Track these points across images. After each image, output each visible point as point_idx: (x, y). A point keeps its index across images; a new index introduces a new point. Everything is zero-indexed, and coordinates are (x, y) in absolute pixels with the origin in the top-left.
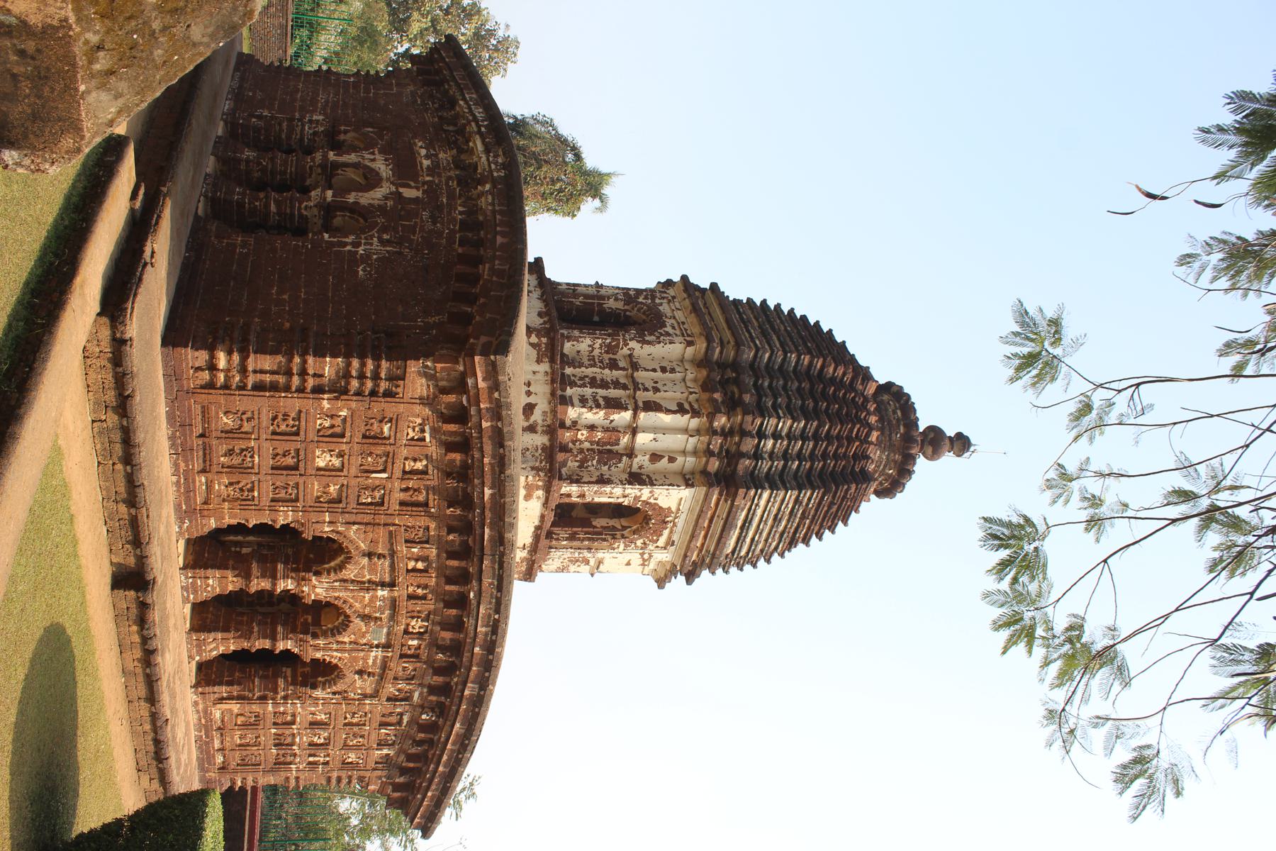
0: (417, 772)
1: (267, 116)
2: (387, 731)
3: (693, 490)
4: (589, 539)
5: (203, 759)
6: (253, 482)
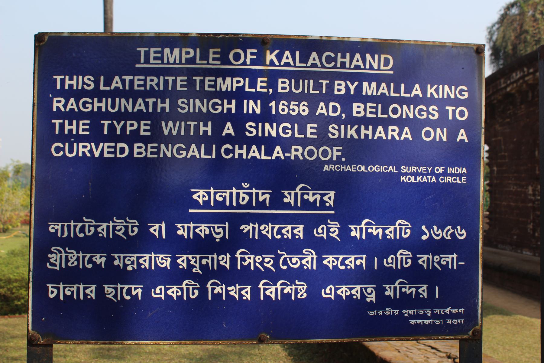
1: (533, 226)
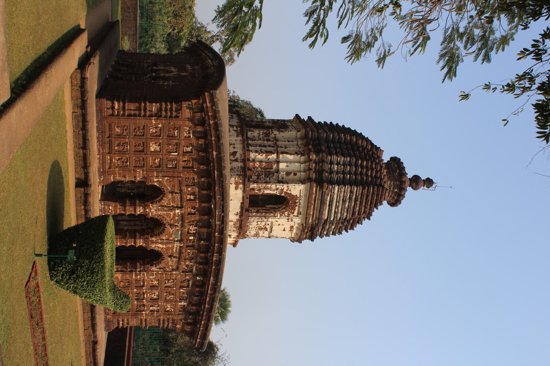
0: (197, 313)
2: (183, 291)
3: (305, 185)
4: (265, 212)
6: (127, 158)
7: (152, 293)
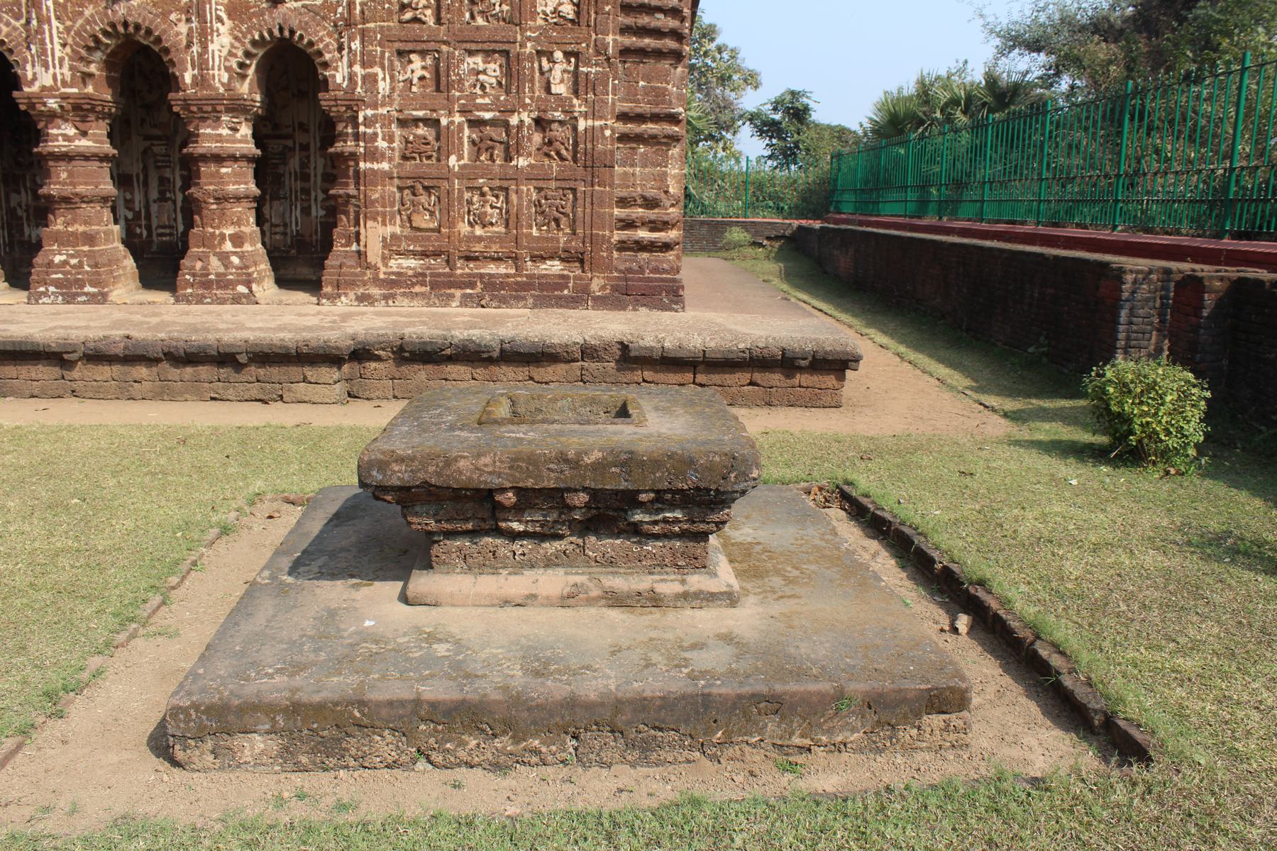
5: (533, 296)
7: (475, 86)
